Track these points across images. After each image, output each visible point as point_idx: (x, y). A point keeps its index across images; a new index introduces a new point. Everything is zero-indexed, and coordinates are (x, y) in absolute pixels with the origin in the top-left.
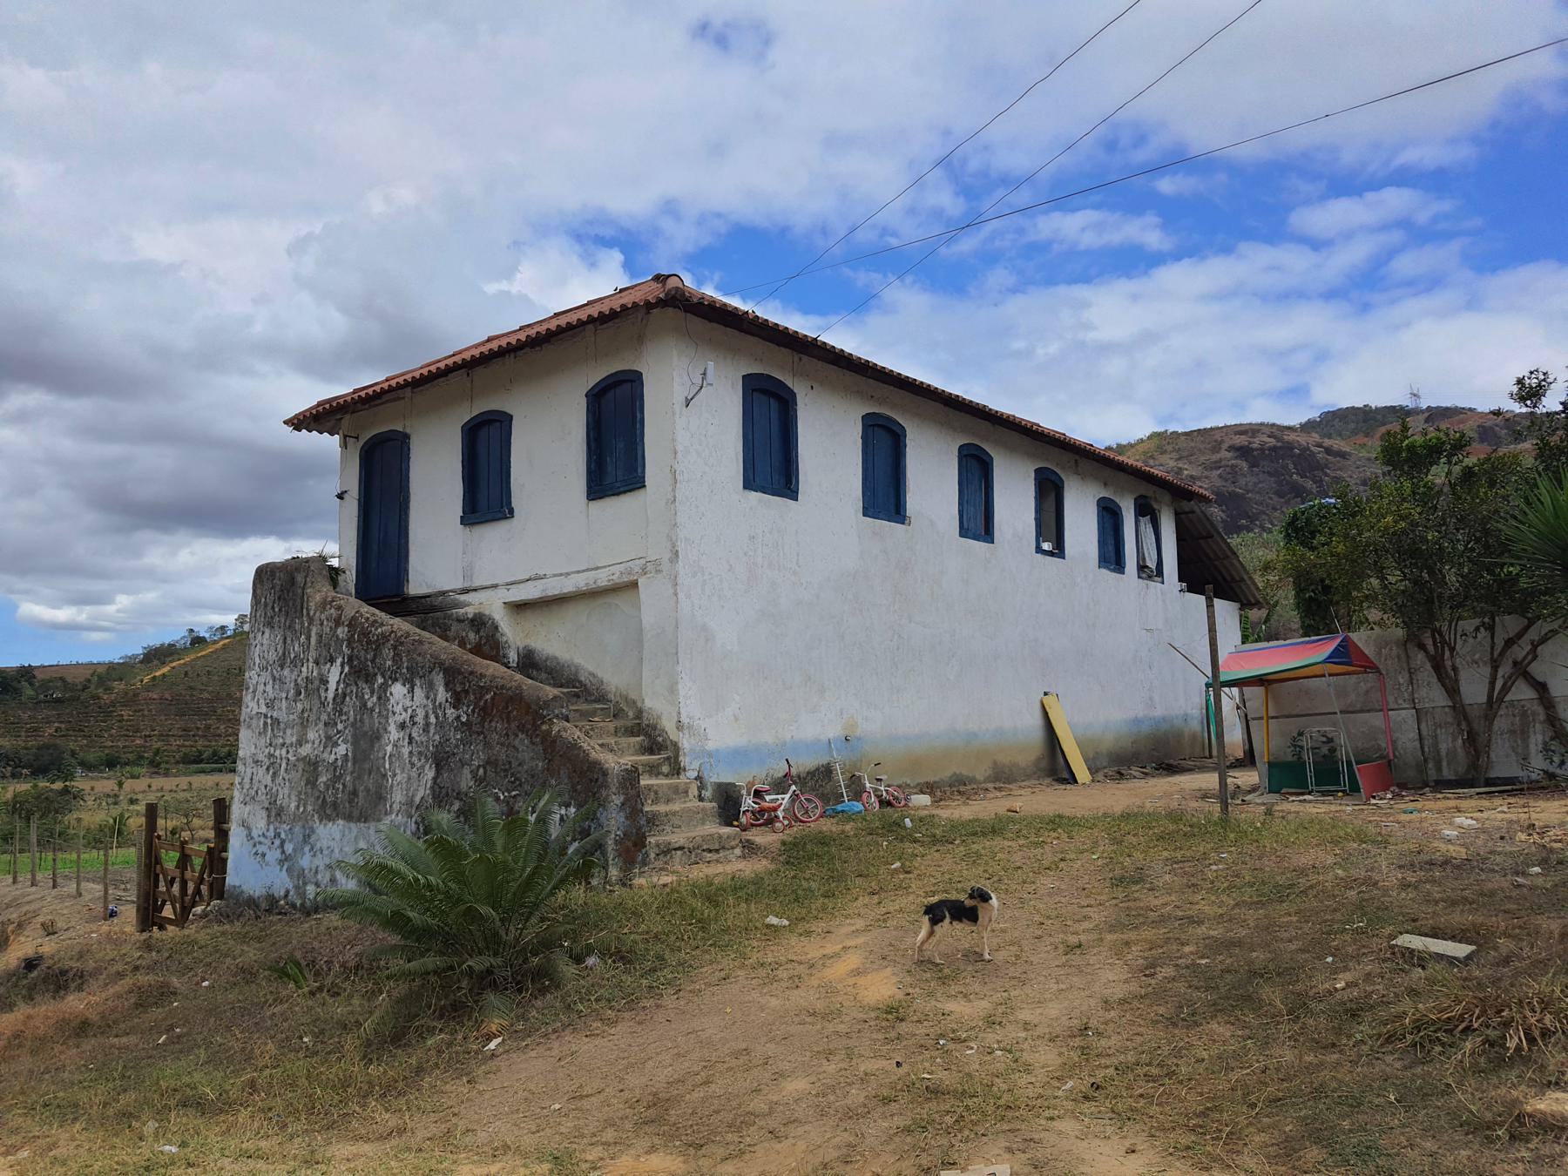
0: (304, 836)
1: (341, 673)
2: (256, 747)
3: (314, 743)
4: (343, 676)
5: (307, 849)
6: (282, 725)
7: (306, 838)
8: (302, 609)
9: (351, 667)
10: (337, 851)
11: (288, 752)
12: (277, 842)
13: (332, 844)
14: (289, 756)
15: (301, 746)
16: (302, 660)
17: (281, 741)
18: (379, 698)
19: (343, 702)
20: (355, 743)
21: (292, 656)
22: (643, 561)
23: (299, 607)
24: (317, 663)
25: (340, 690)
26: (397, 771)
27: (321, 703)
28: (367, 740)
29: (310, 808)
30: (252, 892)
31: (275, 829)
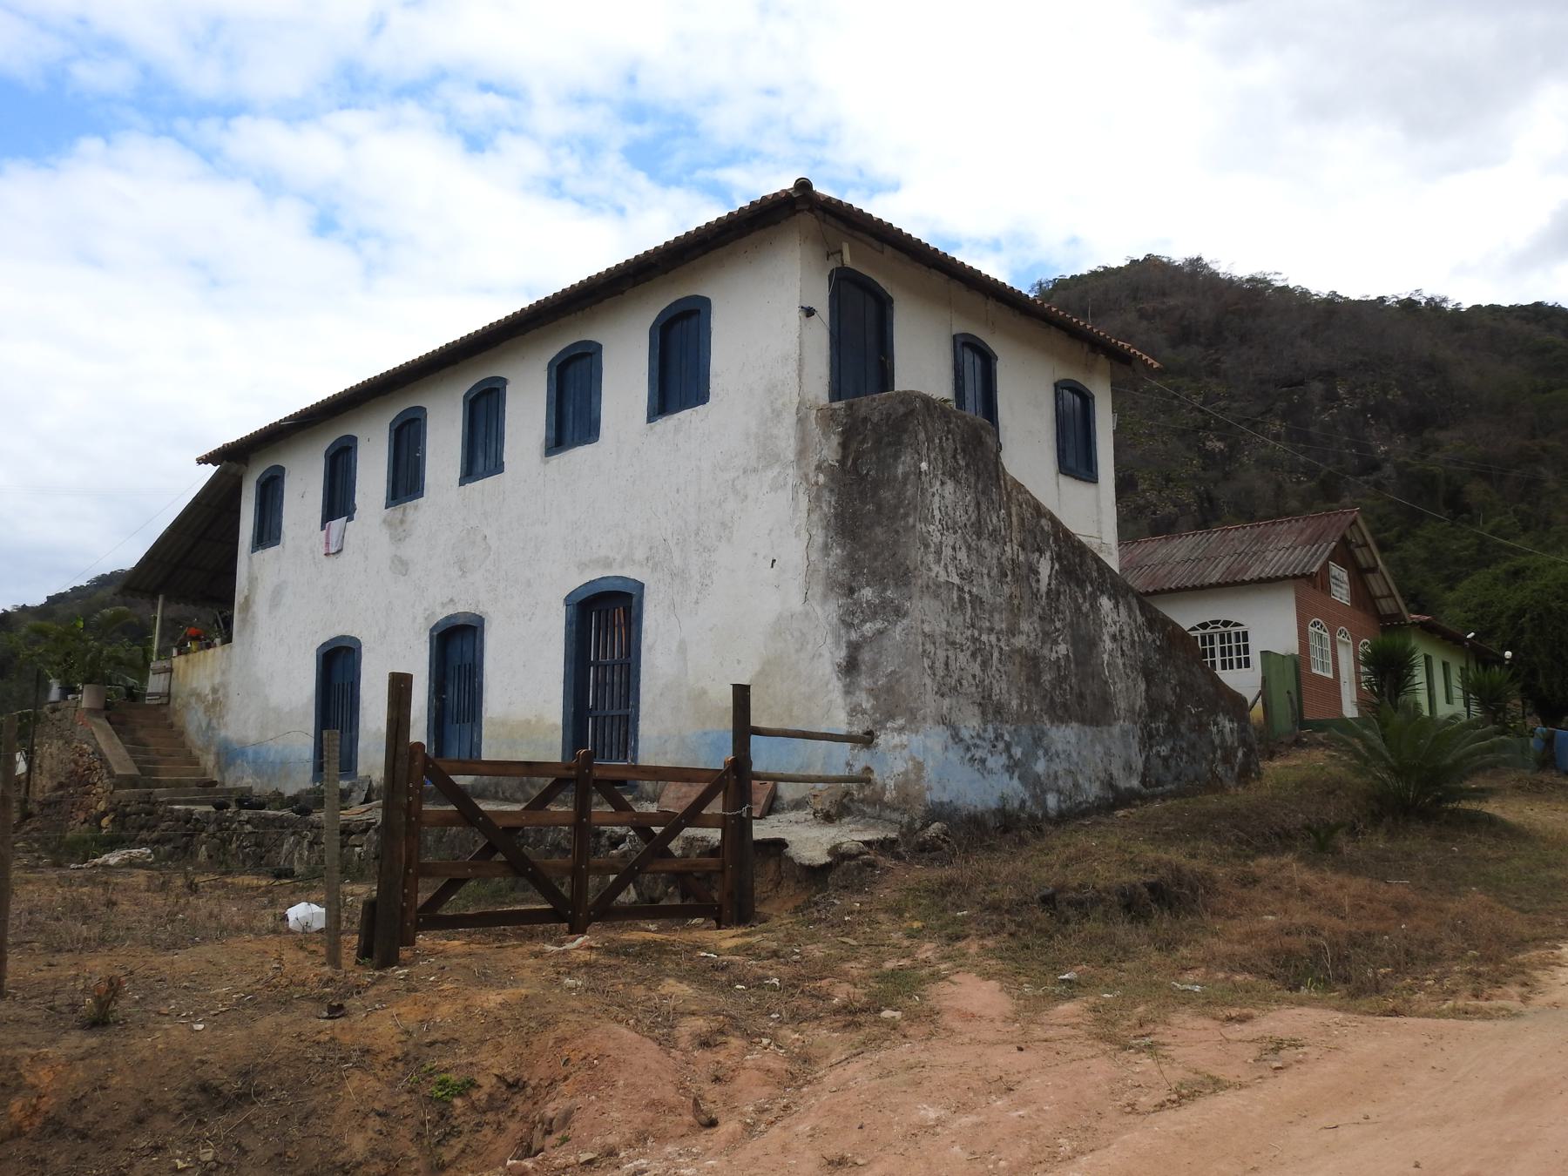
0: (1034, 739)
1: (1052, 568)
2: (948, 625)
3: (1029, 636)
4: (1054, 572)
5: (1040, 753)
6: (987, 607)
7: (1038, 740)
8: (998, 476)
9: (1061, 565)
10: (1074, 755)
11: (999, 640)
12: (1001, 746)
13: (1068, 748)
14: (1002, 644)
15: (1014, 635)
16: (1004, 538)
17: (988, 624)
18: (1091, 606)
19: (1058, 600)
20: (1076, 641)
21: (991, 528)
22: (1099, 541)
23: (994, 474)
24: (1022, 546)
25: (1053, 586)
26: (1116, 679)
27: (1032, 593)
28: (1085, 645)
29: (1035, 707)
30: (972, 808)
31: (995, 730)
